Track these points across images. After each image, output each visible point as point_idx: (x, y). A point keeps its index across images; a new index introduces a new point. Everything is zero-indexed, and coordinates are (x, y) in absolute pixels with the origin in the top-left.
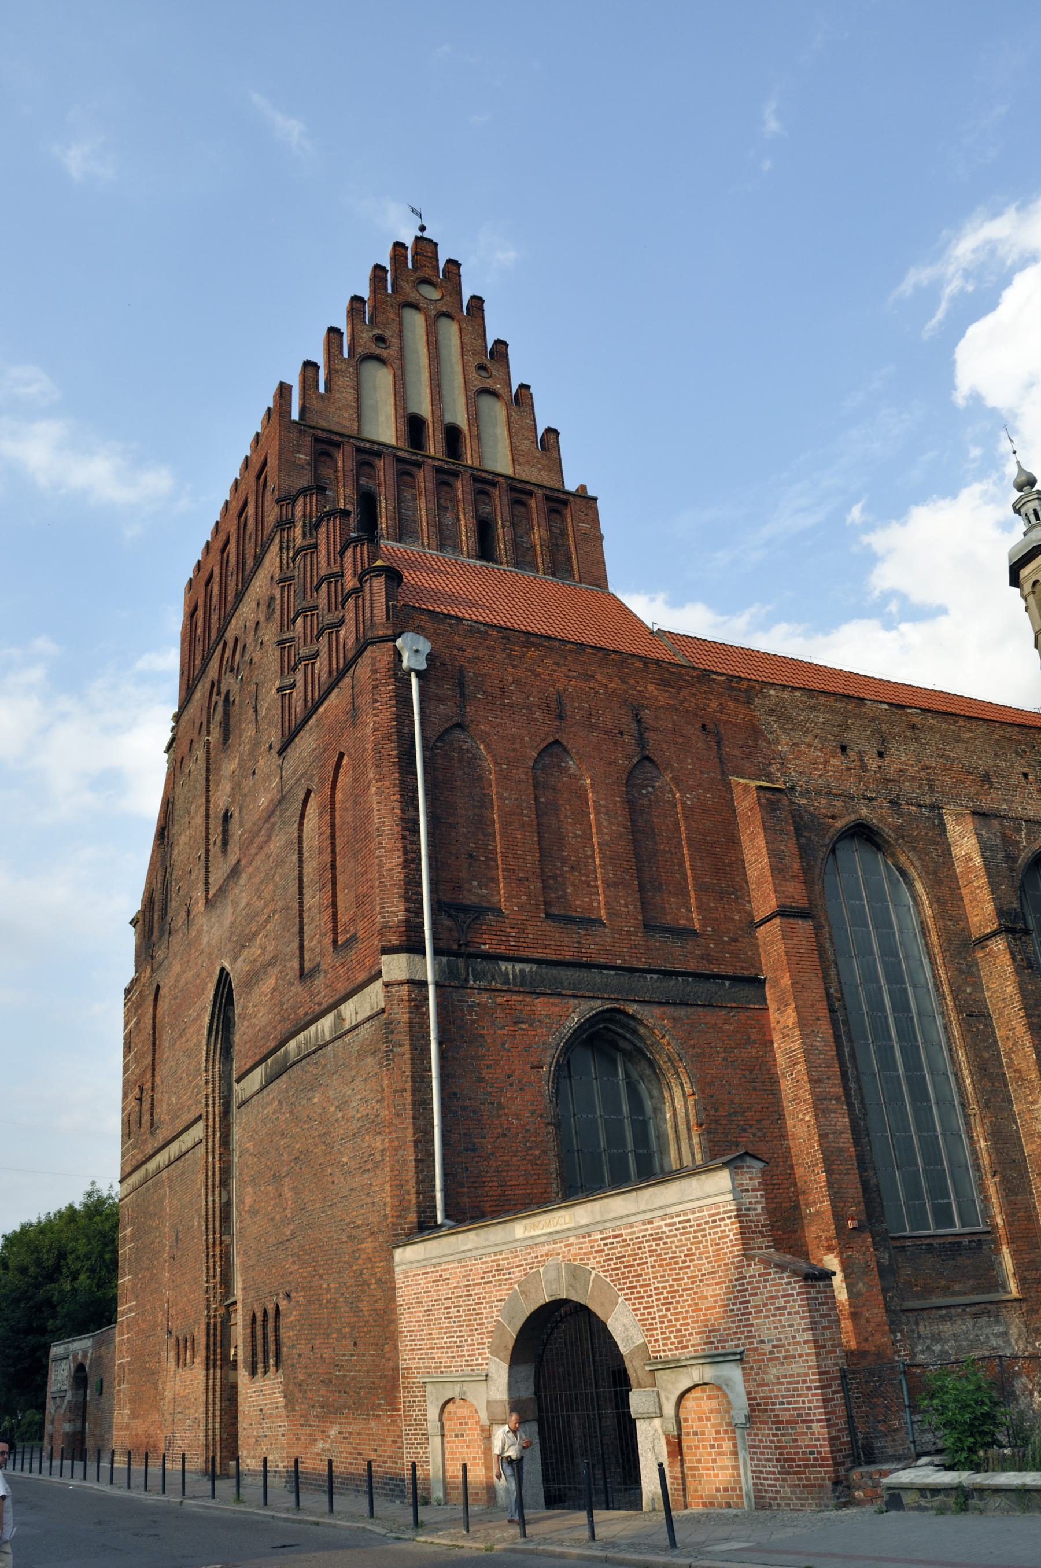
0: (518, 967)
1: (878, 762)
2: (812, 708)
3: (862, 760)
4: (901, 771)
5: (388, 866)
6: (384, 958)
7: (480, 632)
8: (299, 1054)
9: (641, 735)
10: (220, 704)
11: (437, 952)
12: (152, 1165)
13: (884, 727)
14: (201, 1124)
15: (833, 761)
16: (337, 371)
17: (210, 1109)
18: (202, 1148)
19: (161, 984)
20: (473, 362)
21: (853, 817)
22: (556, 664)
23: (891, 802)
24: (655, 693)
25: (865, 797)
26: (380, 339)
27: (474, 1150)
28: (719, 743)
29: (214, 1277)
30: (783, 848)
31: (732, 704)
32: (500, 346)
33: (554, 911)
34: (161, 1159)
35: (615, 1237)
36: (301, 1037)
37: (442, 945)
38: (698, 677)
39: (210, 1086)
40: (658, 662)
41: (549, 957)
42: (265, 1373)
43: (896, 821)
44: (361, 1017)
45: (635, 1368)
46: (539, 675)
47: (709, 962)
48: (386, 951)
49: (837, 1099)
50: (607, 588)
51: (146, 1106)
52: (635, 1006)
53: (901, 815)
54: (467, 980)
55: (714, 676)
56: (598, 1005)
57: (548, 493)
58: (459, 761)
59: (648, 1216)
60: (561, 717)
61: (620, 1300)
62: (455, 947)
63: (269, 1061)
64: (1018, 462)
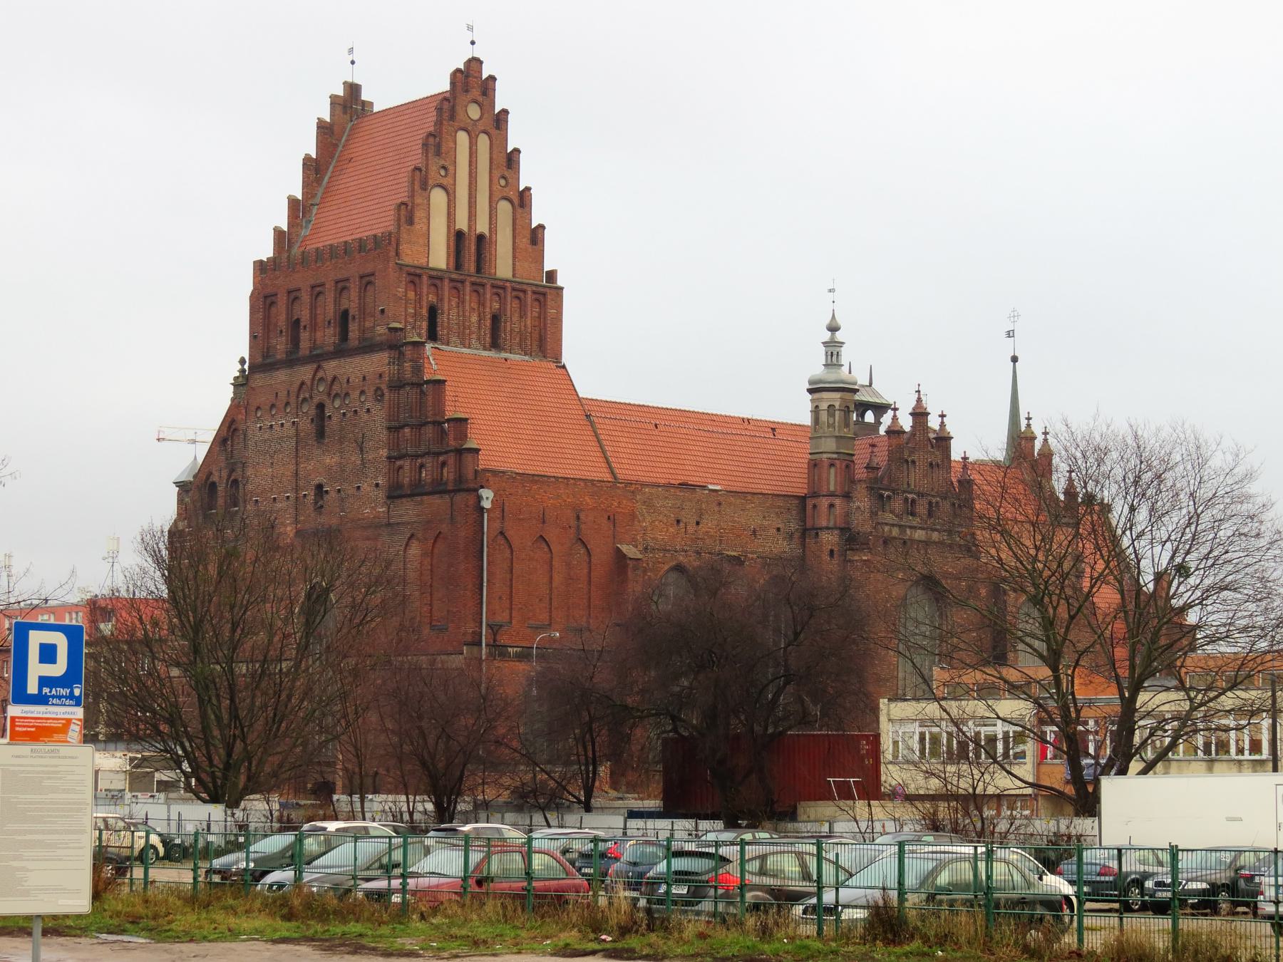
0: (515, 649)
4: (707, 532)
15: (671, 530)
24: (589, 501)
25: (683, 550)
60: (544, 522)
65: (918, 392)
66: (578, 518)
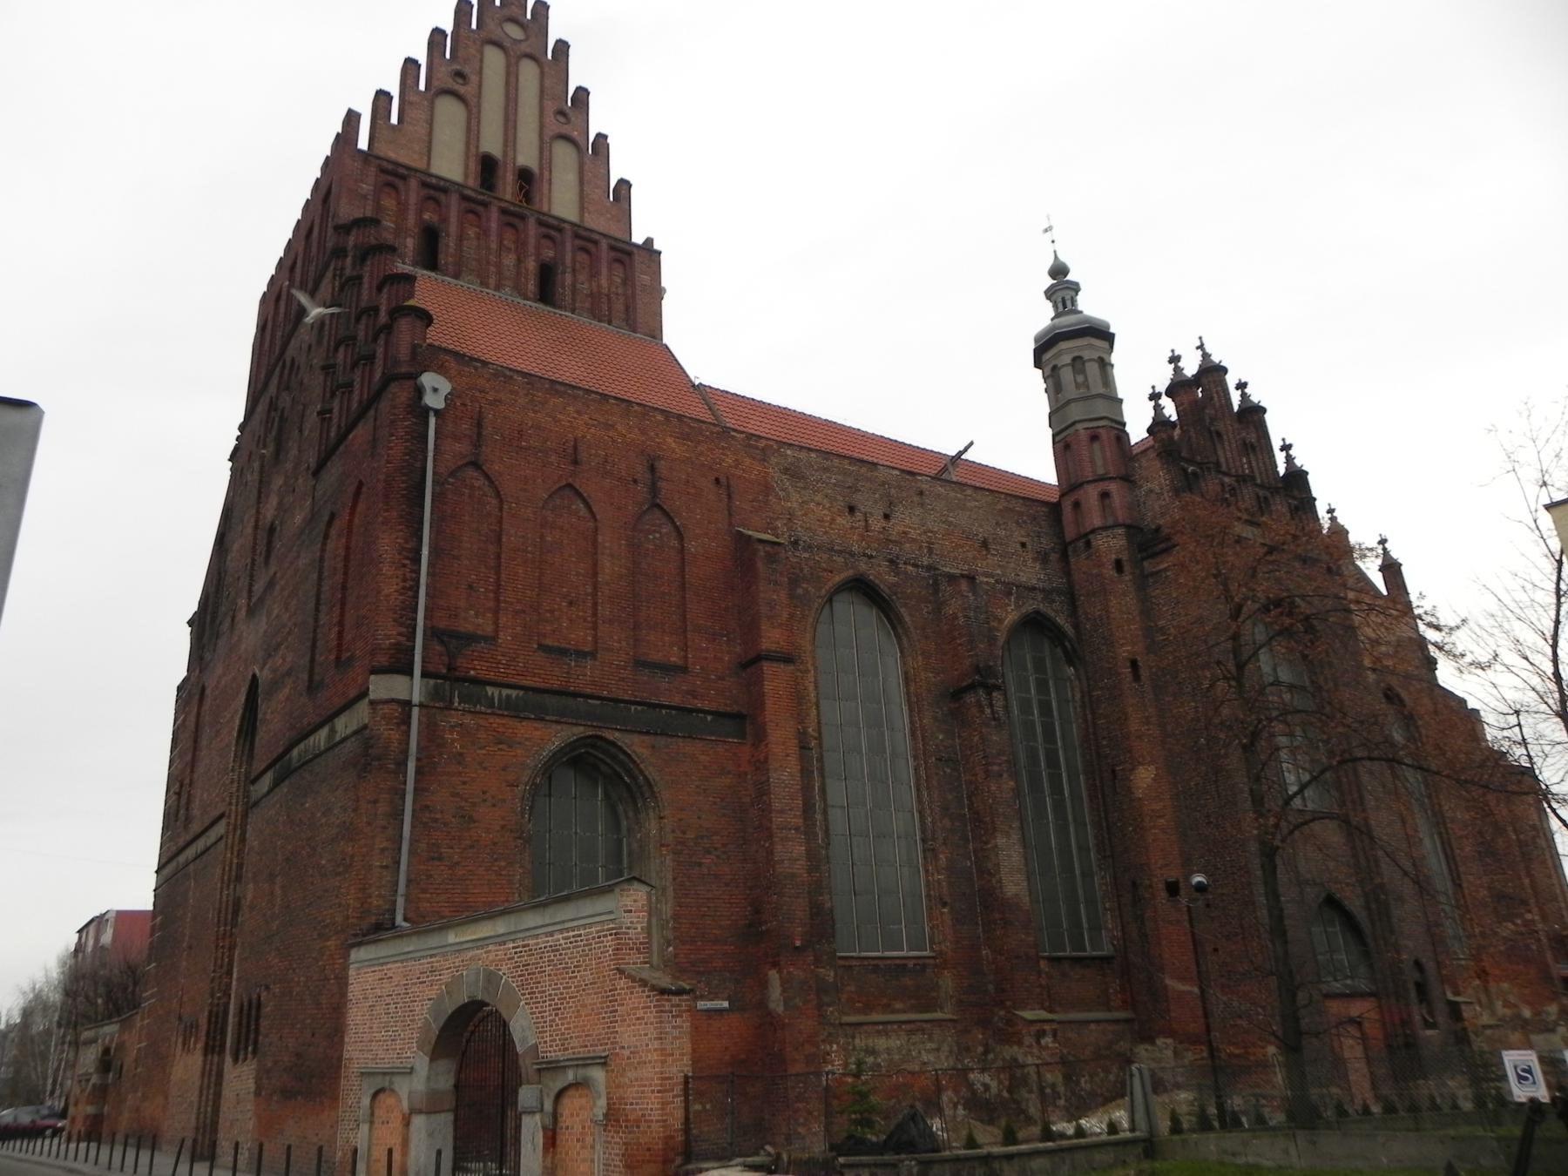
0: (505, 692)
1: (883, 523)
2: (826, 470)
3: (866, 521)
4: (904, 532)
5: (386, 592)
6: (372, 677)
7: (505, 376)
8: (299, 761)
9: (654, 484)
10: (277, 419)
11: (424, 675)
12: (182, 858)
13: (893, 491)
14: (223, 822)
15: (839, 520)
16: (411, 103)
17: (233, 808)
18: (221, 845)
19: (206, 684)
20: (550, 107)
21: (851, 572)
22: (578, 412)
23: (891, 561)
24: (673, 445)
25: (865, 555)
26: (460, 74)
27: (440, 859)
28: (729, 497)
29: (221, 967)
30: (775, 597)
31: (748, 461)
32: (581, 93)
33: (548, 642)
34: (190, 853)
35: (524, 946)
36: (302, 746)
37: (431, 668)
38: (718, 433)
39: (235, 785)
40: (680, 417)
41: (538, 685)
42: (245, 1059)
43: (892, 579)
44: (349, 731)
45: (527, 1066)
46: (559, 421)
47: (695, 697)
48: (375, 671)
49: (797, 829)
50: (662, 340)
51: (183, 801)
52: (617, 734)
53: (897, 574)
54: (452, 702)
55: (733, 433)
56: (579, 731)
57: (613, 243)
58: (470, 496)
59: (550, 929)
60: (575, 462)
61: (522, 1003)
62: (444, 671)
63: (277, 766)
64: (1055, 252)
65: (1201, 347)
66: (652, 469)
